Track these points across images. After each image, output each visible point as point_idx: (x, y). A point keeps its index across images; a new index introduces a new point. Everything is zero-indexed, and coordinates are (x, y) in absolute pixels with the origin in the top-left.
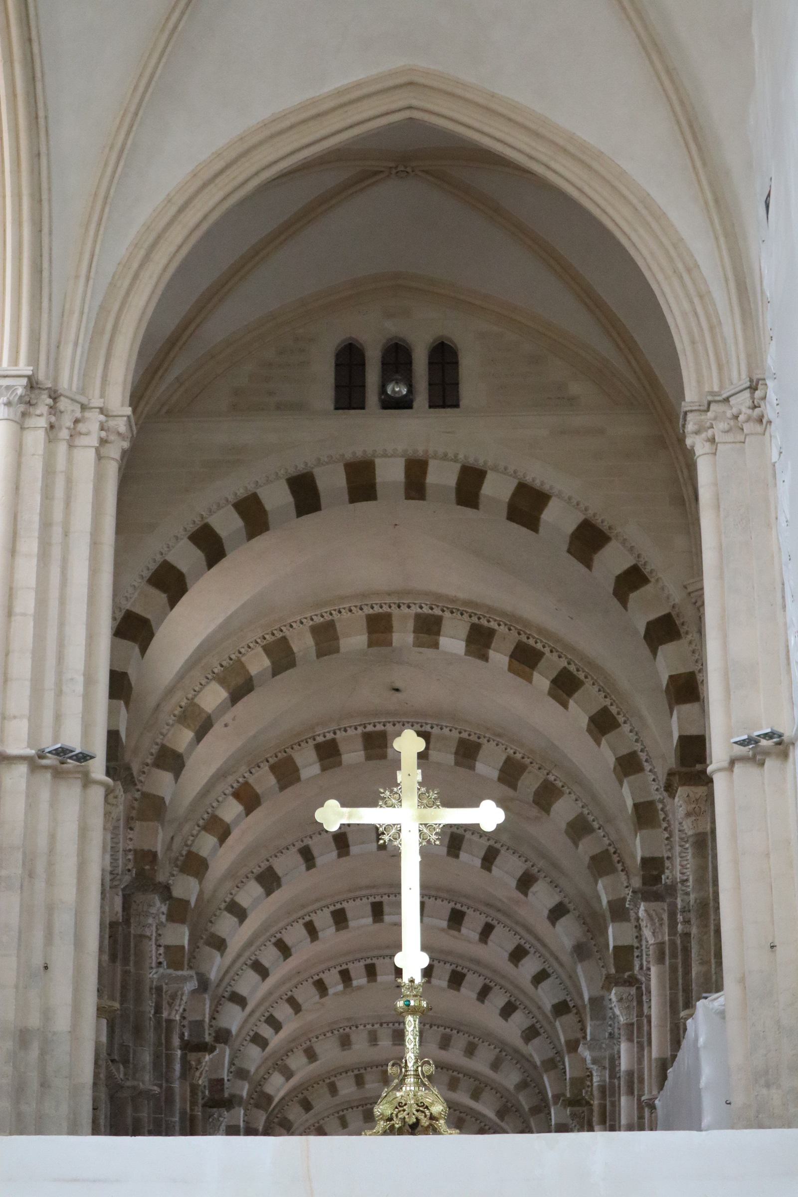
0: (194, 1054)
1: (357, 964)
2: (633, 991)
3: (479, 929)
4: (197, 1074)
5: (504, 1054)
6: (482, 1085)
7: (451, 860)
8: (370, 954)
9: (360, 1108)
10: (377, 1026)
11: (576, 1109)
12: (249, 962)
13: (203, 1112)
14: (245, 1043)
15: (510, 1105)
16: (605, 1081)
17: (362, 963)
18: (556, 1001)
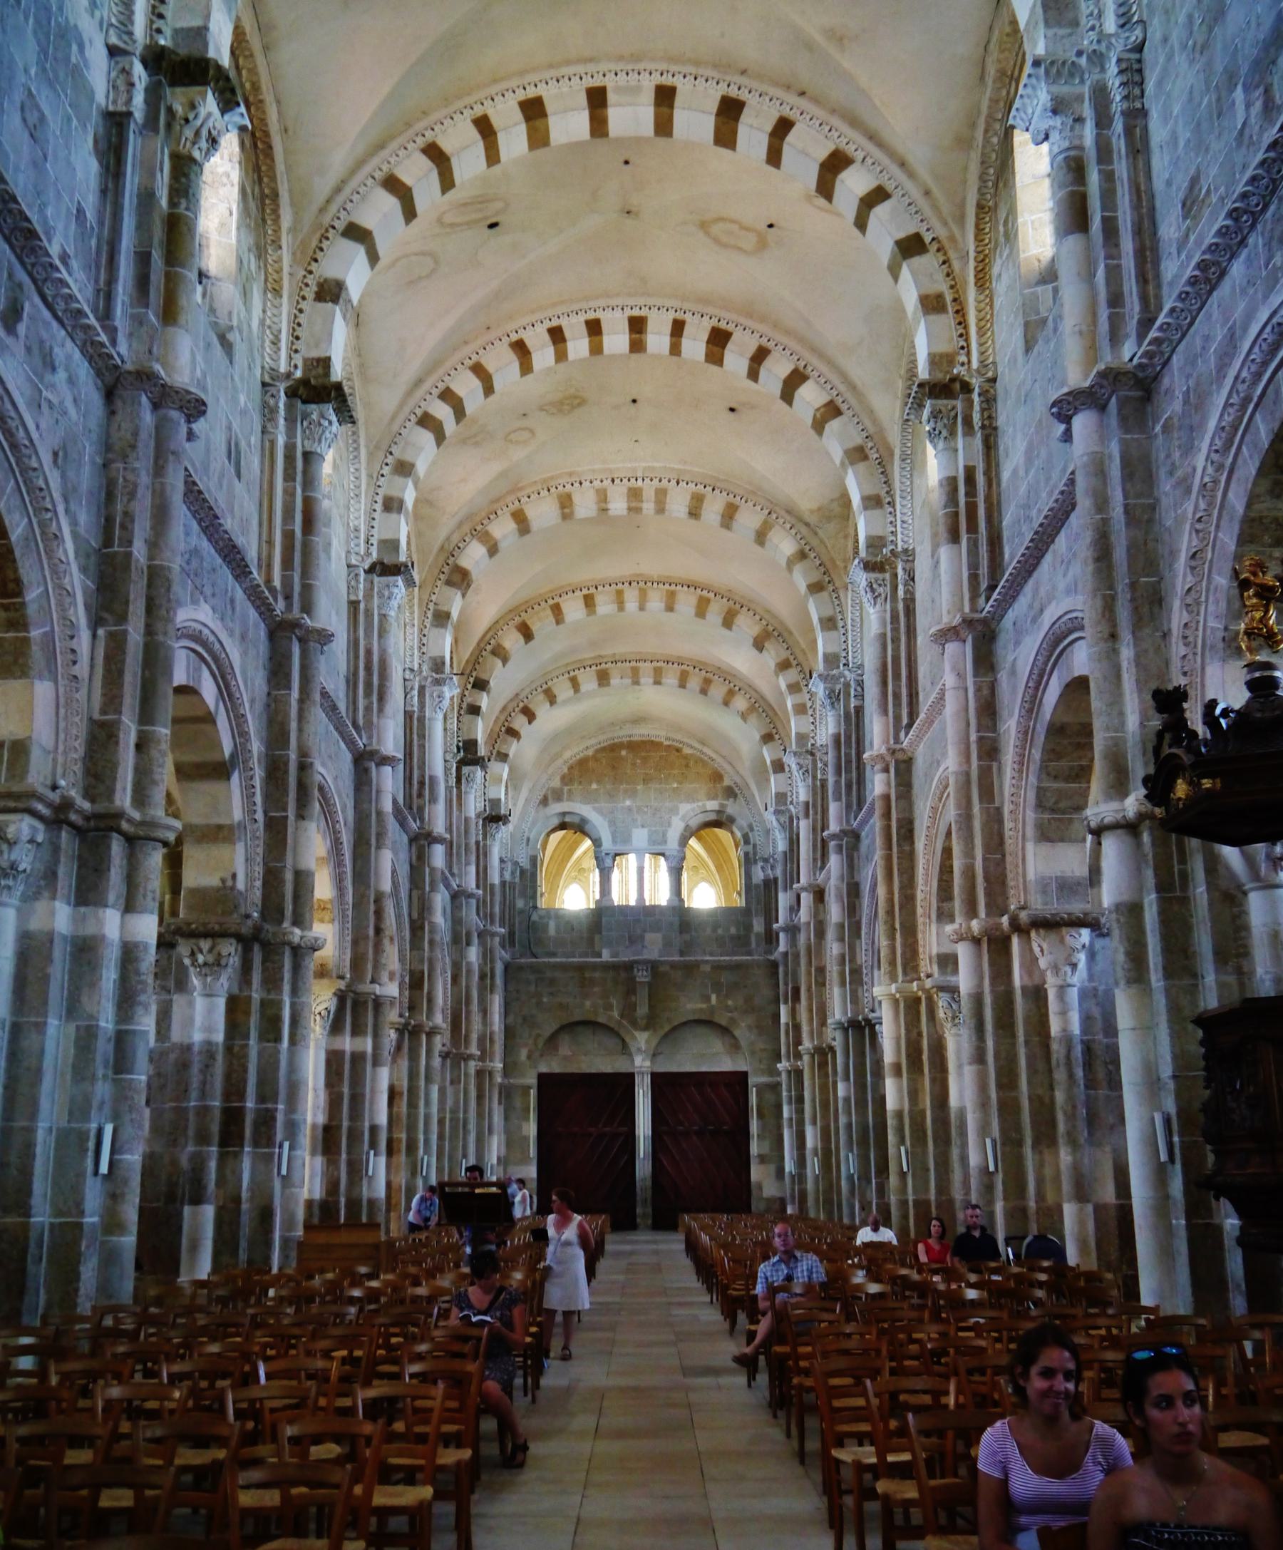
0: (179, 90)
3: (769, 128)
4: (189, 133)
5: (774, 516)
6: (738, 606)
8: (593, 304)
9: (594, 667)
10: (607, 483)
11: (942, 403)
12: (378, 175)
13: (290, 408)
14: (408, 424)
15: (770, 628)
16: (1081, 148)
17: (582, 318)
18: (901, 235)
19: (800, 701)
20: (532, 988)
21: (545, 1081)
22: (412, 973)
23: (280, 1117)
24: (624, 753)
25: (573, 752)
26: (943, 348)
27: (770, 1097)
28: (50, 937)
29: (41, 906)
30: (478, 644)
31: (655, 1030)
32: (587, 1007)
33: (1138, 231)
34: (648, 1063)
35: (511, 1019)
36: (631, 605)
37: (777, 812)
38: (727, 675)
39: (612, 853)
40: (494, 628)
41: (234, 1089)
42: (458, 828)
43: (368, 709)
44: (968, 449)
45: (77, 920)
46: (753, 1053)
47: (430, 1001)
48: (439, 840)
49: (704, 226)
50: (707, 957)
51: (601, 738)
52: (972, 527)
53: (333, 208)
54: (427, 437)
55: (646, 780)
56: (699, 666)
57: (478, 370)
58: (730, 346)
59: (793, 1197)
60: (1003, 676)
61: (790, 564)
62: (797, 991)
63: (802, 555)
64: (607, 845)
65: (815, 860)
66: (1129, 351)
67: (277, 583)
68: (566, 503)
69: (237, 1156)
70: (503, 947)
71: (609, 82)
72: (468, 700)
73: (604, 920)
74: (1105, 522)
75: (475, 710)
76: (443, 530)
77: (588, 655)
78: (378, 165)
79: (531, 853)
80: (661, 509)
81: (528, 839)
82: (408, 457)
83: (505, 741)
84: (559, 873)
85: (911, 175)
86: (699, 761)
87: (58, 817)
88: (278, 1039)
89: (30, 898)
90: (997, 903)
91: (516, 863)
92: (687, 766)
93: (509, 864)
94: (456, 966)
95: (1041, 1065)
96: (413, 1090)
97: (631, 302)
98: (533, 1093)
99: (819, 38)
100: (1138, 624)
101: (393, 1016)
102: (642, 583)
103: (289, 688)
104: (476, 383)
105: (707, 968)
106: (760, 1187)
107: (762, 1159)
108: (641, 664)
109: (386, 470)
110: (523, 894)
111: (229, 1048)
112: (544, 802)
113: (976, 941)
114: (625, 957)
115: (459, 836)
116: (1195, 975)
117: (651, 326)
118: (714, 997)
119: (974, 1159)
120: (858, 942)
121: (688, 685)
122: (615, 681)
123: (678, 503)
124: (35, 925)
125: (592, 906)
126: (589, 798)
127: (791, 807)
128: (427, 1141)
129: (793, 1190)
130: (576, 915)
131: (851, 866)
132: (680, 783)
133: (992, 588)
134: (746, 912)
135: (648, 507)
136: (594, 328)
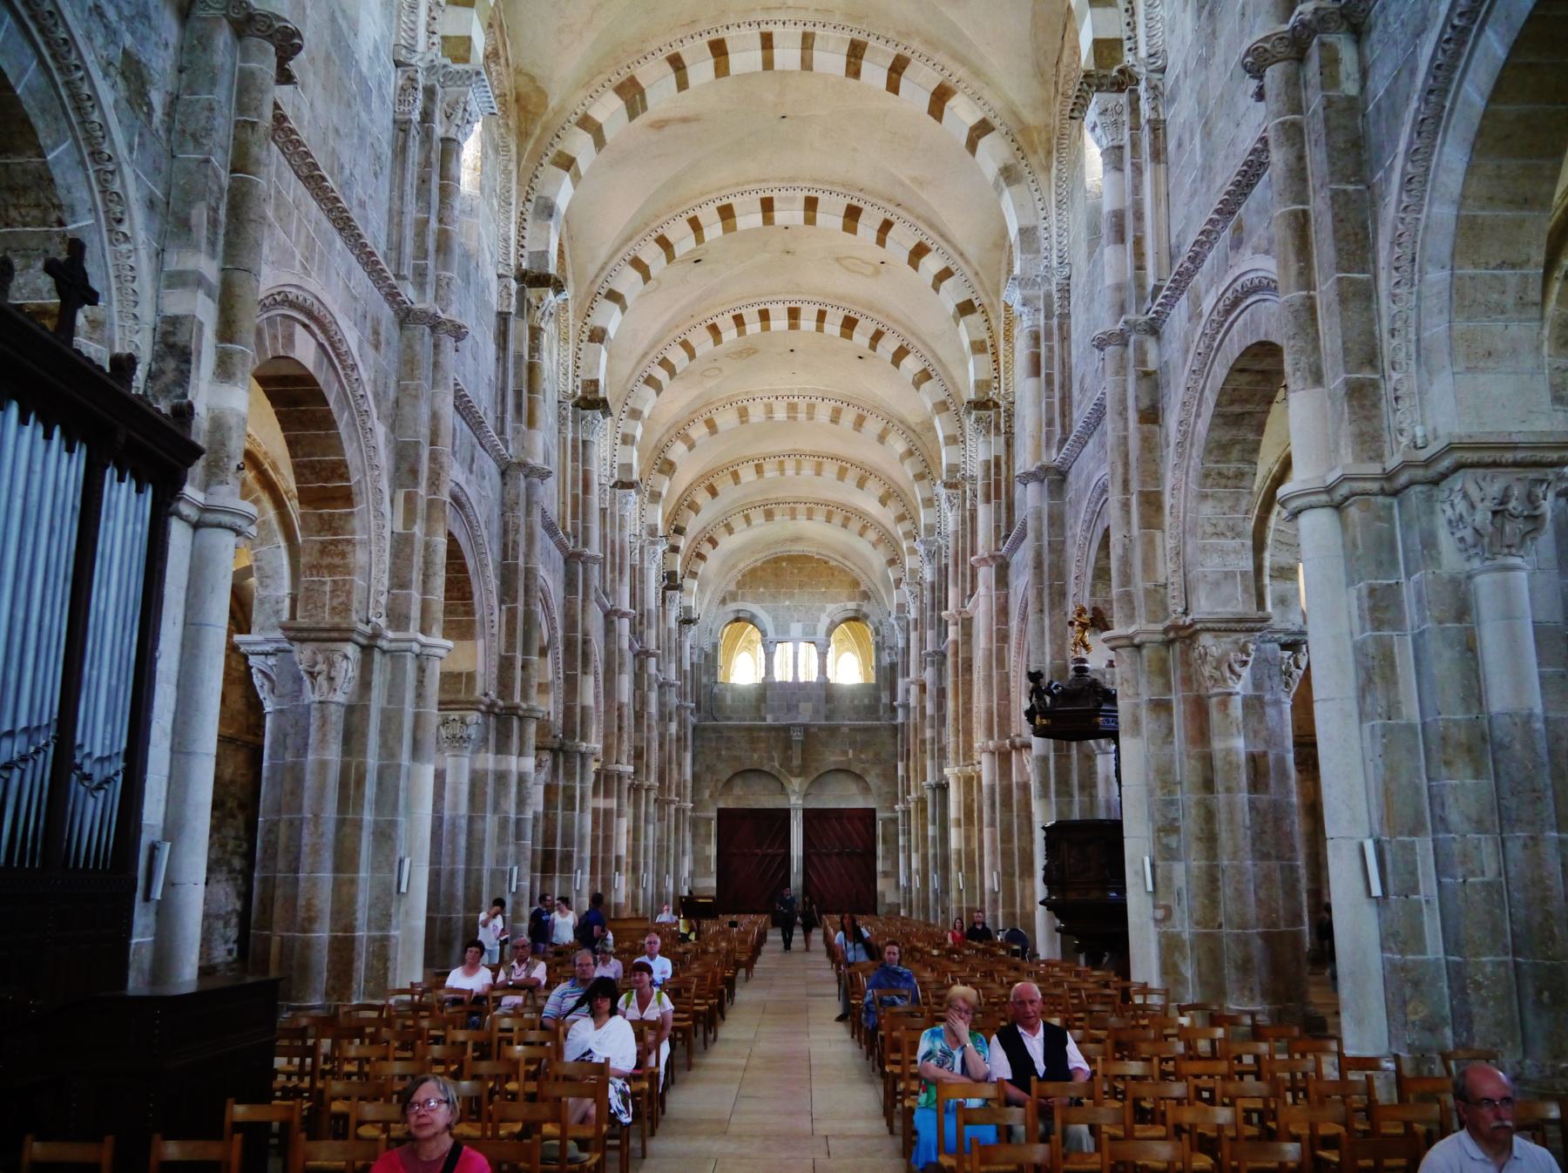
1: (750, 309)
2: (1124, 98)
4: (539, 314)
7: (852, 82)
12: (628, 258)
13: (574, 413)
17: (756, 308)
18: (960, 300)
21: (722, 813)
23: (575, 855)
25: (744, 565)
26: (984, 376)
28: (486, 772)
29: (481, 755)
32: (755, 759)
33: (1062, 386)
36: (790, 472)
37: (897, 618)
38: (861, 514)
40: (690, 489)
41: (549, 839)
43: (613, 581)
44: (997, 445)
45: (497, 762)
46: (879, 795)
47: (648, 767)
48: (652, 655)
49: (838, 260)
52: (998, 496)
53: (600, 281)
54: (650, 392)
55: (801, 586)
56: (841, 507)
57: (685, 345)
58: (857, 329)
60: (1012, 591)
61: (902, 459)
63: (910, 453)
64: (771, 635)
66: (1054, 457)
67: (569, 529)
68: (743, 414)
69: (552, 878)
71: (775, 194)
74: (1041, 547)
76: (659, 431)
78: (627, 252)
80: (811, 416)
82: (637, 407)
84: (733, 648)
85: (967, 262)
86: (842, 571)
87: (490, 710)
88: (573, 809)
89: (476, 751)
90: (1004, 733)
94: (662, 736)
95: (1026, 830)
97: (790, 297)
98: (714, 824)
99: (907, 182)
100: (1052, 606)
101: (627, 782)
102: (798, 456)
103: (576, 593)
104: (684, 354)
105: (846, 730)
107: (886, 874)
109: (623, 416)
110: (707, 672)
111: (546, 815)
112: (723, 601)
113: (993, 753)
116: (1071, 795)
117: (803, 315)
119: (987, 884)
123: (823, 412)
124: (479, 765)
125: (759, 681)
126: (757, 599)
128: (646, 864)
130: (747, 688)
131: (940, 675)
133: (1007, 536)
134: (877, 687)
135: (802, 416)
136: (764, 316)
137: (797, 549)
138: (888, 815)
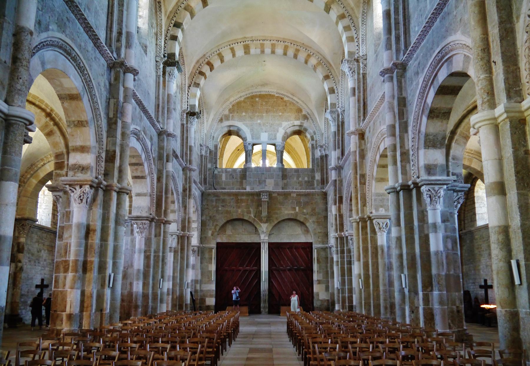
19: (350, 35)
20: (214, 204)
21: (220, 246)
22: (107, 151)
24: (257, 99)
25: (234, 98)
27: (323, 254)
30: (177, 4)
31: (270, 223)
32: (238, 212)
34: (267, 238)
35: (204, 218)
37: (332, 112)
39: (252, 144)
42: (163, 99)
46: (315, 234)
50: (295, 189)
51: (247, 92)
55: (267, 112)
59: (339, 300)
62: (341, 198)
64: (249, 140)
65: (359, 117)
70: (201, 184)
72: (172, 33)
73: (247, 173)
75: (174, 38)
77: (239, 36)
79: (214, 143)
81: (213, 137)
83: (198, 78)
86: (291, 103)
91: (208, 147)
92: (286, 105)
93: (204, 147)
96: (104, 230)
98: (214, 251)
106: (318, 295)
107: (319, 282)
108: (265, 42)
110: (211, 161)
112: (221, 120)
114: (257, 189)
115: (163, 103)
118: (297, 208)
120: (406, 135)
121: (288, 53)
122: (252, 51)
126: (241, 119)
127: (339, 109)
129: (339, 296)
132: (283, 113)
134: (313, 170)
137: (265, 90)
138: (320, 246)
